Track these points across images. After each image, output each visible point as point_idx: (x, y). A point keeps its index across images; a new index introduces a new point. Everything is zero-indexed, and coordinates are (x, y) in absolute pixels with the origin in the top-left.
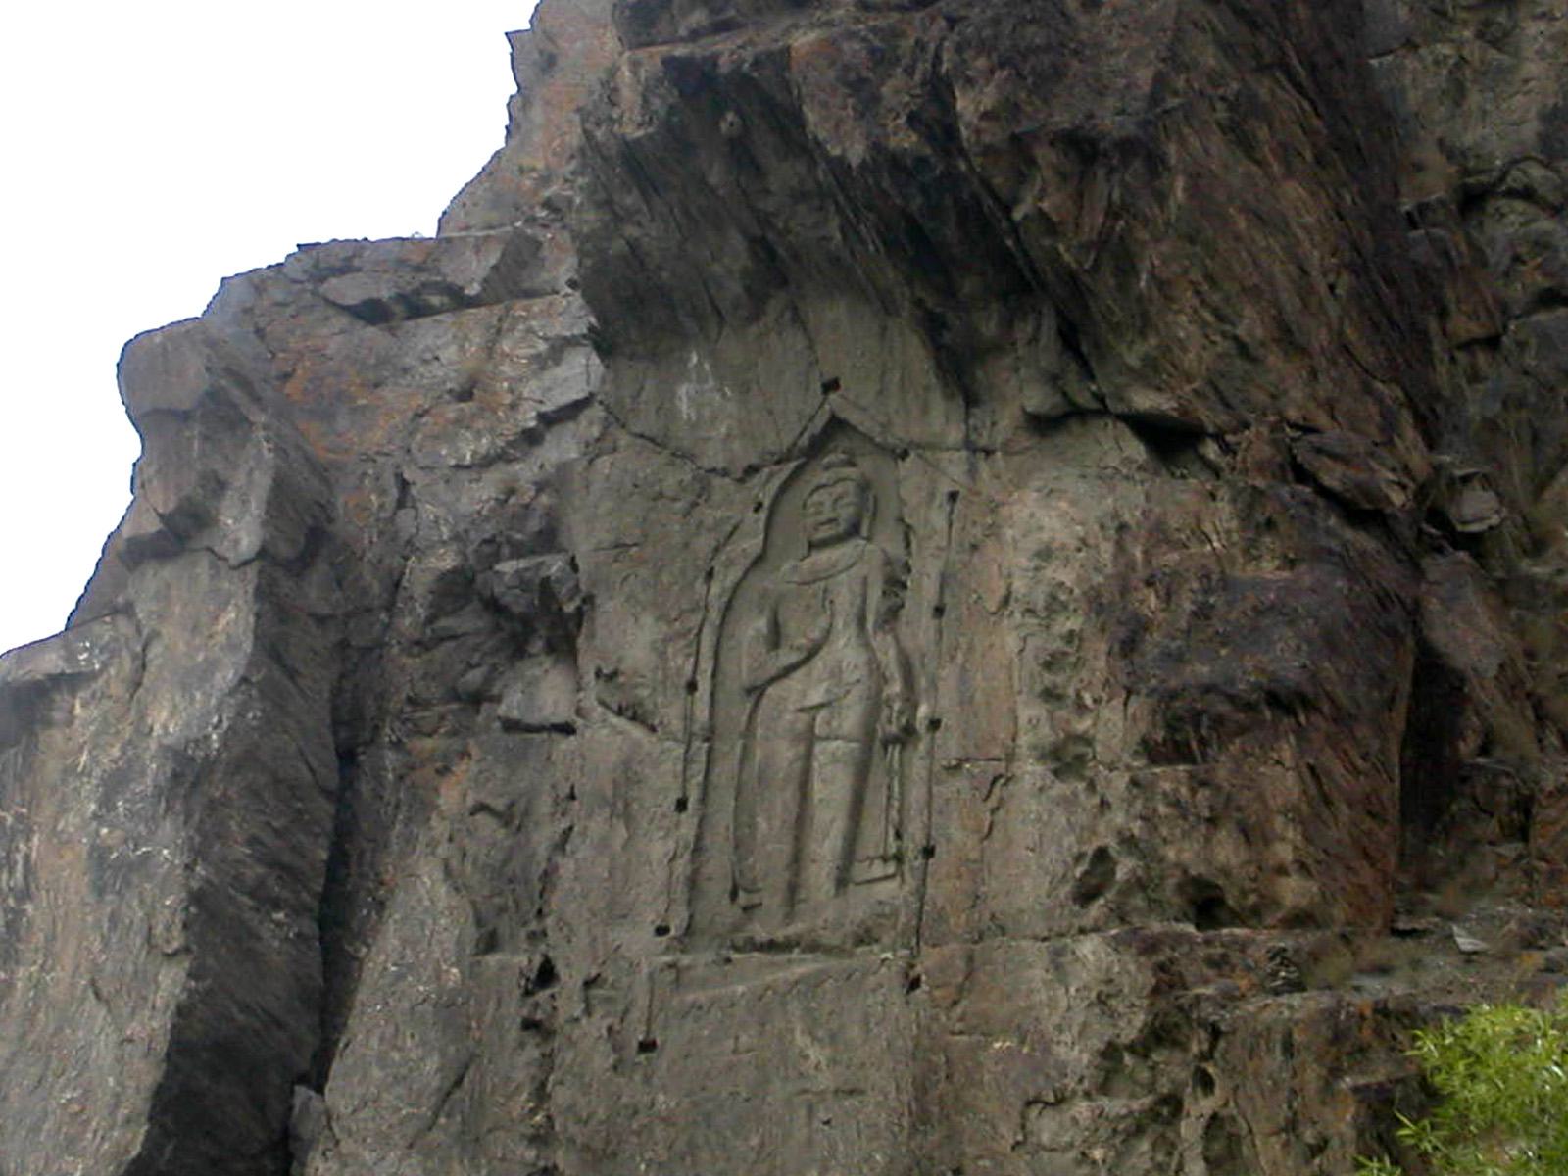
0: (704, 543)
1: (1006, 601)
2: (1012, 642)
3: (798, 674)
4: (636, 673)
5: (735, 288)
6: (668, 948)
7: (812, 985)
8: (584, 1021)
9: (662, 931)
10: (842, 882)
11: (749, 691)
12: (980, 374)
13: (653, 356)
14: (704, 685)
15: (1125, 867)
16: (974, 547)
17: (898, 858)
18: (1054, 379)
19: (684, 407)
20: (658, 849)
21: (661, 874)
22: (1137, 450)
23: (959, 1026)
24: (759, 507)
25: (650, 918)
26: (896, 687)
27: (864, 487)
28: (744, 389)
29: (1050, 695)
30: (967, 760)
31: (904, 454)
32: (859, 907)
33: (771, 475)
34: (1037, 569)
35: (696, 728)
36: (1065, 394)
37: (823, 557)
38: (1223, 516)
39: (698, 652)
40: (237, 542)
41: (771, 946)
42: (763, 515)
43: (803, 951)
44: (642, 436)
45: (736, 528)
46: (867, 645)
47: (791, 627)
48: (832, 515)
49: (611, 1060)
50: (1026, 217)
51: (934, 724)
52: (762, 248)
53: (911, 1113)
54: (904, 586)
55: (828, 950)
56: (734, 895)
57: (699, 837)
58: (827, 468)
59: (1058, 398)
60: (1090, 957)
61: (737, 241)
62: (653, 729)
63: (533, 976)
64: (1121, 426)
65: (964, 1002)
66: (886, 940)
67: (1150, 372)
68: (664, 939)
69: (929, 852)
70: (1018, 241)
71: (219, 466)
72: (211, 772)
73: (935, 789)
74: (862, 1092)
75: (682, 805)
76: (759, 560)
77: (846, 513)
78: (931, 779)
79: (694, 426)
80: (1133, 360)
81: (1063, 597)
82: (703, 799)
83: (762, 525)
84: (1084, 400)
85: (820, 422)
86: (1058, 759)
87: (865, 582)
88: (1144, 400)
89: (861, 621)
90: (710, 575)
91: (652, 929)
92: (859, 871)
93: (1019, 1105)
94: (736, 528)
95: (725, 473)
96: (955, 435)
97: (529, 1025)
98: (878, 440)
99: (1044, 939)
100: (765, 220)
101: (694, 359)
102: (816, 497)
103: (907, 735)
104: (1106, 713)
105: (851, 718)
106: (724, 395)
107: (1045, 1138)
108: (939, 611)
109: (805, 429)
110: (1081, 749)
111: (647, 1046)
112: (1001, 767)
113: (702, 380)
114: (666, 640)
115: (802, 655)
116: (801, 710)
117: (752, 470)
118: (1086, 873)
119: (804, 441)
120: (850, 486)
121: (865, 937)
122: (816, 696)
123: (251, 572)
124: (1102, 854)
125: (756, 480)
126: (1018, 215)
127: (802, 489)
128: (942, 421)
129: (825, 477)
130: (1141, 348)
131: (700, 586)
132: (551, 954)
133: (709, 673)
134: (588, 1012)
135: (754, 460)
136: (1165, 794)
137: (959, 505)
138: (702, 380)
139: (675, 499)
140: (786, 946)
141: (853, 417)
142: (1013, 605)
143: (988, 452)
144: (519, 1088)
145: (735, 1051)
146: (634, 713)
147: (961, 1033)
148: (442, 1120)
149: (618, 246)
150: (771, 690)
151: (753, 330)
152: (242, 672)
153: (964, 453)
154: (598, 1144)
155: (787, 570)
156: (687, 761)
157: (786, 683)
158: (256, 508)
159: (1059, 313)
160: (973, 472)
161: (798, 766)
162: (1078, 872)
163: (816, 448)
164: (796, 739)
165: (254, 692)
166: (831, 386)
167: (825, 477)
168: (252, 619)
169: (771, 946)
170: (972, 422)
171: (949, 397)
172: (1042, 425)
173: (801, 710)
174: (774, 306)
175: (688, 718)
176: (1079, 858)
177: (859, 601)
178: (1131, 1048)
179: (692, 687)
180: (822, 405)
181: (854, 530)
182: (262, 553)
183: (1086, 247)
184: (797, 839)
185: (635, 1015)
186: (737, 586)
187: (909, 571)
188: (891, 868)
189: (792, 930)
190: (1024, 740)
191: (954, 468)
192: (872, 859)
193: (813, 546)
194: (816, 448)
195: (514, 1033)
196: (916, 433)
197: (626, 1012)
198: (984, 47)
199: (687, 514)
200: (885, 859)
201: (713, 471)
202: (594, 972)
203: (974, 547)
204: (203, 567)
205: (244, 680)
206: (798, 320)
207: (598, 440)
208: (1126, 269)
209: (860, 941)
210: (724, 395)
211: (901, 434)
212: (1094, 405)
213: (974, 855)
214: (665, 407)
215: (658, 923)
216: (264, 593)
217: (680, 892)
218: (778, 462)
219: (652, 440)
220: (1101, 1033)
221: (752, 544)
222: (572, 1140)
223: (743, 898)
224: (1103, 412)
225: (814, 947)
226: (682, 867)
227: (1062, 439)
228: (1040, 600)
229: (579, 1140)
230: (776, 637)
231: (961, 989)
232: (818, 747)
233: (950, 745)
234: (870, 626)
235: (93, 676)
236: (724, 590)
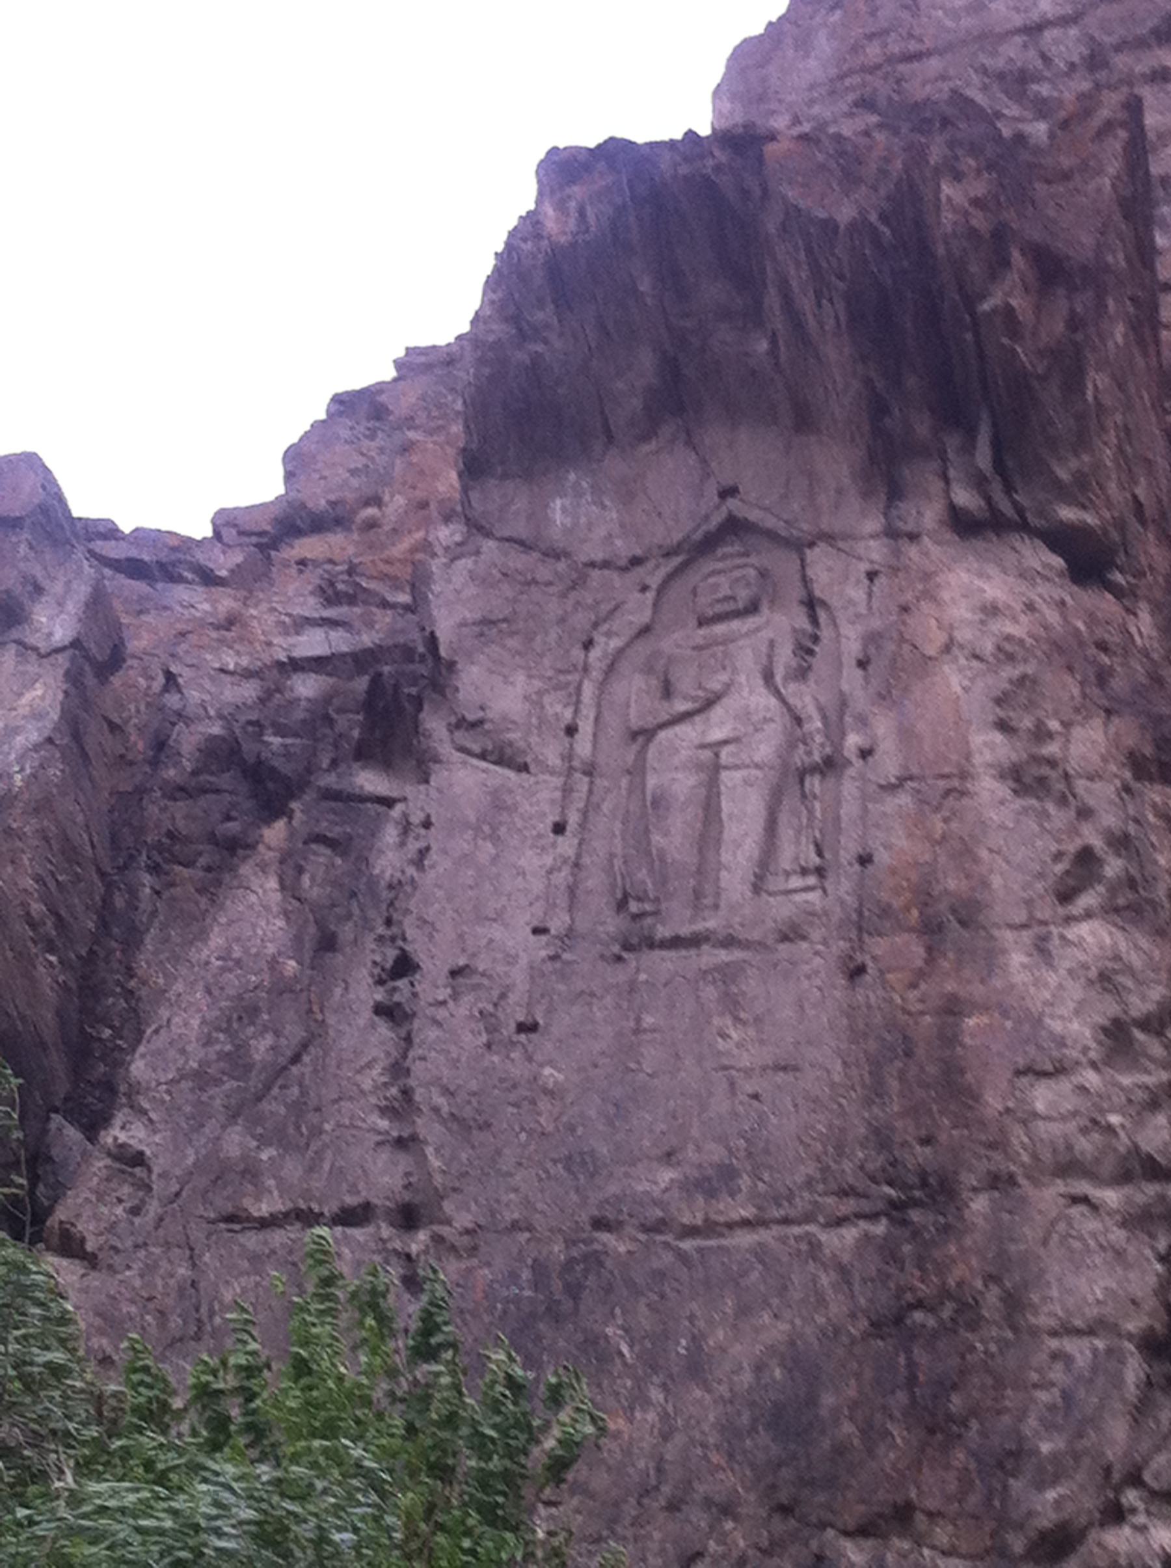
0: (582, 620)
1: (947, 648)
2: (956, 682)
3: (697, 719)
4: (504, 718)
6: (547, 944)
7: (727, 975)
8: (451, 1004)
9: (537, 931)
10: (757, 889)
11: (634, 735)
12: (907, 472)
13: (528, 475)
14: (586, 727)
15: (1113, 867)
16: (905, 609)
17: (820, 872)
18: (979, 482)
19: (558, 517)
20: (532, 861)
21: (537, 886)
22: (1058, 562)
23: (920, 1007)
24: (644, 589)
25: (523, 920)
27: (763, 574)
29: (1003, 726)
30: (911, 778)
31: (811, 545)
32: (781, 910)
33: (657, 566)
34: (982, 622)
35: (576, 763)
36: (989, 500)
37: (720, 629)
38: (1144, 625)
39: (578, 702)
40: (50, 634)
41: (676, 942)
42: (650, 595)
43: (713, 946)
44: (509, 540)
45: (617, 607)
46: (777, 693)
47: (685, 681)
48: (729, 593)
49: (484, 1038)
50: (994, 311)
51: (865, 754)
53: (864, 1086)
54: (810, 652)
55: (745, 945)
56: (621, 906)
57: (579, 856)
58: (724, 557)
59: (983, 503)
60: (1090, 939)
61: (646, 360)
62: (524, 768)
63: (388, 966)
64: (1038, 542)
65: (923, 986)
66: (816, 934)
67: (1080, 489)
68: (544, 938)
69: (865, 860)
70: (977, 334)
71: (38, 572)
72: (11, 806)
73: (870, 806)
74: (796, 1069)
75: (559, 828)
76: (645, 630)
77: (743, 595)
78: (865, 798)
79: (568, 531)
80: (1063, 474)
81: (1008, 647)
82: (583, 825)
83: (650, 602)
84: (1005, 507)
85: (717, 519)
86: (1018, 780)
87: (772, 644)
88: (1067, 513)
89: (768, 677)
90: (588, 645)
91: (528, 930)
92: (775, 883)
93: (1009, 1075)
94: (617, 607)
95: (606, 564)
96: (873, 524)
98: (783, 533)
99: (1024, 926)
101: (572, 476)
102: (711, 580)
103: (831, 765)
104: (1077, 732)
105: (765, 748)
106: (604, 507)
107: (1040, 1106)
108: (862, 664)
109: (699, 526)
110: (1045, 771)
112: (956, 783)
113: (579, 494)
114: (540, 693)
115: (697, 705)
116: (703, 746)
117: (636, 561)
118: (1067, 872)
119: (698, 536)
120: (752, 572)
121: (791, 934)
122: (717, 735)
123: (62, 660)
124: (1086, 857)
125: (640, 571)
126: (986, 306)
127: (693, 577)
129: (720, 565)
130: (1074, 464)
131: (577, 653)
132: (407, 948)
133: (592, 716)
134: (455, 996)
135: (639, 552)
136: (1154, 805)
137: (882, 581)
138: (579, 494)
139: (549, 584)
141: (754, 515)
142: (955, 650)
143: (913, 537)
144: (369, 1065)
145: (637, 1031)
146: (503, 756)
147: (922, 1013)
148: (275, 1091)
150: (662, 735)
151: (646, 448)
152: (46, 733)
153: (885, 540)
154: (468, 1112)
155: (676, 640)
156: (567, 790)
157: (679, 729)
158: (73, 607)
159: (995, 425)
160: (897, 553)
161: (703, 791)
162: (1059, 868)
163: (707, 545)
164: (699, 767)
165: (58, 755)
166: (728, 492)
167: (720, 565)
168: (61, 696)
169: (676, 942)
170: (894, 512)
171: (866, 495)
172: (963, 525)
173: (703, 746)
174: (666, 431)
175: (568, 756)
176: (1058, 856)
177: (764, 661)
178: (1144, 1024)
179: (571, 730)
180: (718, 507)
182: (76, 644)
183: (1040, 353)
184: (700, 851)
185: (512, 998)
186: (620, 652)
187: (816, 639)
188: (812, 880)
189: (699, 927)
190: (977, 760)
191: (876, 551)
192: (788, 874)
193: (700, 624)
194: (707, 545)
195: (367, 1014)
196: (824, 525)
197: (503, 996)
198: (974, 149)
199: (563, 595)
200: (804, 872)
201: (592, 564)
202: (462, 962)
203: (905, 609)
205: (50, 740)
206: (690, 443)
207: (458, 544)
208: (1074, 381)
209: (785, 938)
210: (604, 507)
211: (805, 527)
212: (1016, 517)
213: (927, 857)
215: (535, 923)
216: (73, 678)
217: (562, 901)
218: (667, 555)
219: (522, 543)
220: (1109, 1008)
221: (645, 617)
222: (436, 1110)
223: (634, 907)
224: (1023, 527)
225: (729, 942)
226: (562, 877)
227: (979, 544)
228: (988, 647)
229: (445, 1110)
230: (667, 691)
231: (921, 974)
232: (724, 775)
233: (889, 765)
234: (778, 679)
236: (605, 654)
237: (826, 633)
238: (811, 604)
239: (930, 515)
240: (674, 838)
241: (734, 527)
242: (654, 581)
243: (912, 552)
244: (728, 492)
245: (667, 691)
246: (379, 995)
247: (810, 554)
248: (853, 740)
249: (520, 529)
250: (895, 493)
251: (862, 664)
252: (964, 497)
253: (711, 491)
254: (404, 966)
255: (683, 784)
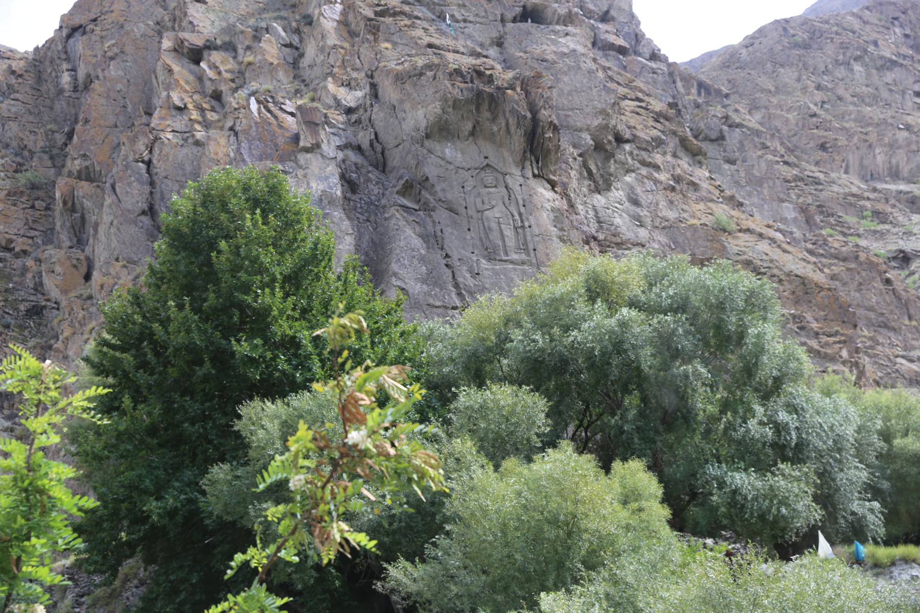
5: (467, 133)
11: (479, 212)
13: (439, 141)
18: (538, 168)
26: (517, 217)
28: (463, 153)
41: (501, 260)
47: (486, 201)
51: (530, 227)
52: (474, 127)
67: (554, 174)
85: (485, 164)
97: (447, 265)
100: (478, 122)
104: (571, 232)
111: (478, 274)
128: (516, 172)
140: (505, 261)
149: (444, 119)
151: (466, 143)
163: (483, 169)
166: (486, 158)
169: (501, 260)
171: (517, 166)
172: (534, 176)
179: (466, 208)
181: (496, 186)
191: (521, 180)
193: (486, 187)
194: (483, 169)
196: (509, 171)
204: (319, 156)
214: (443, 152)
228: (549, 208)
230: (483, 203)
235: (290, 173)
237: (513, 196)
238: (506, 187)
239: (530, 175)
240: (495, 236)
241: (488, 165)
242: (474, 174)
243: (528, 181)
244: (486, 158)
245: (483, 203)
246: (444, 262)
247: (507, 177)
248: (526, 224)
249: (439, 154)
250: (523, 168)
251: (524, 206)
252: (536, 172)
253: (482, 157)
254: (447, 256)
255: (494, 226)
